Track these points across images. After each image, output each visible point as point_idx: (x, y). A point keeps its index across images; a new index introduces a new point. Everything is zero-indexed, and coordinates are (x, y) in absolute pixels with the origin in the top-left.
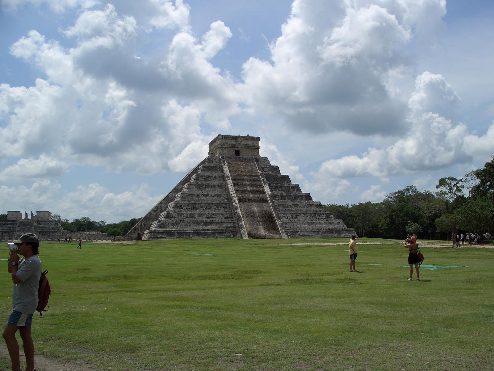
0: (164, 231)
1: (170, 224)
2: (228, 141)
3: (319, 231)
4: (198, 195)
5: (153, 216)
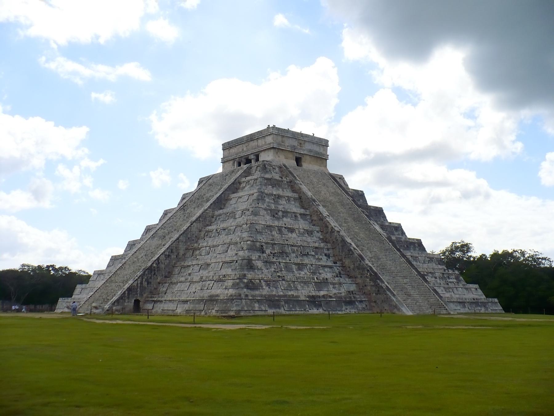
0: (261, 296)
1: (263, 283)
2: (284, 139)
3: (465, 302)
4: (280, 229)
5: (163, 266)
